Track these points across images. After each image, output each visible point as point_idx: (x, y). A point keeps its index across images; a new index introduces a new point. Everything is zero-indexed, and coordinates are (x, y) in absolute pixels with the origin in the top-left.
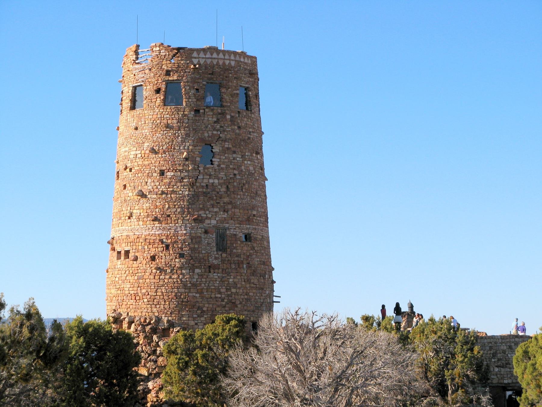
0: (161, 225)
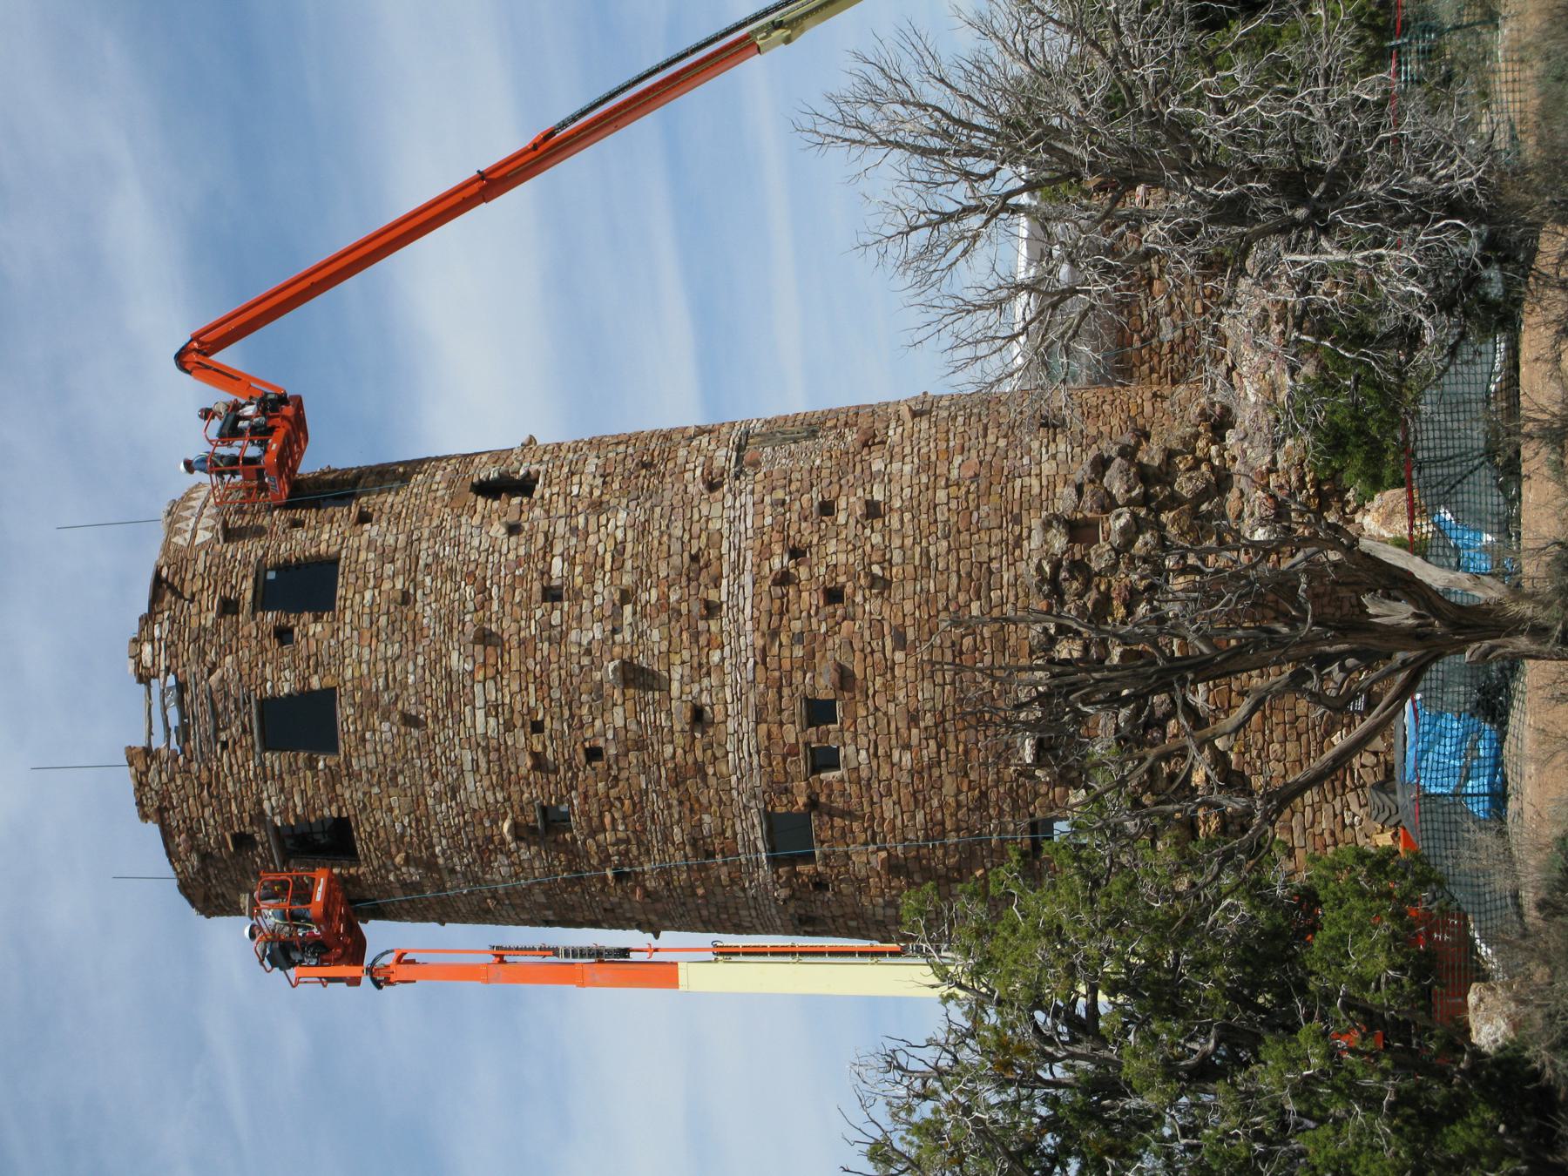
0: (724, 582)
